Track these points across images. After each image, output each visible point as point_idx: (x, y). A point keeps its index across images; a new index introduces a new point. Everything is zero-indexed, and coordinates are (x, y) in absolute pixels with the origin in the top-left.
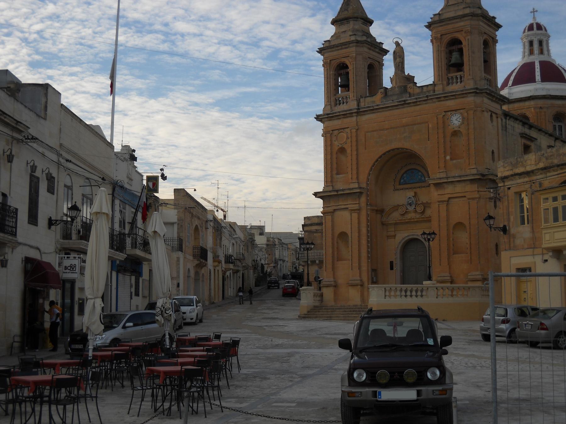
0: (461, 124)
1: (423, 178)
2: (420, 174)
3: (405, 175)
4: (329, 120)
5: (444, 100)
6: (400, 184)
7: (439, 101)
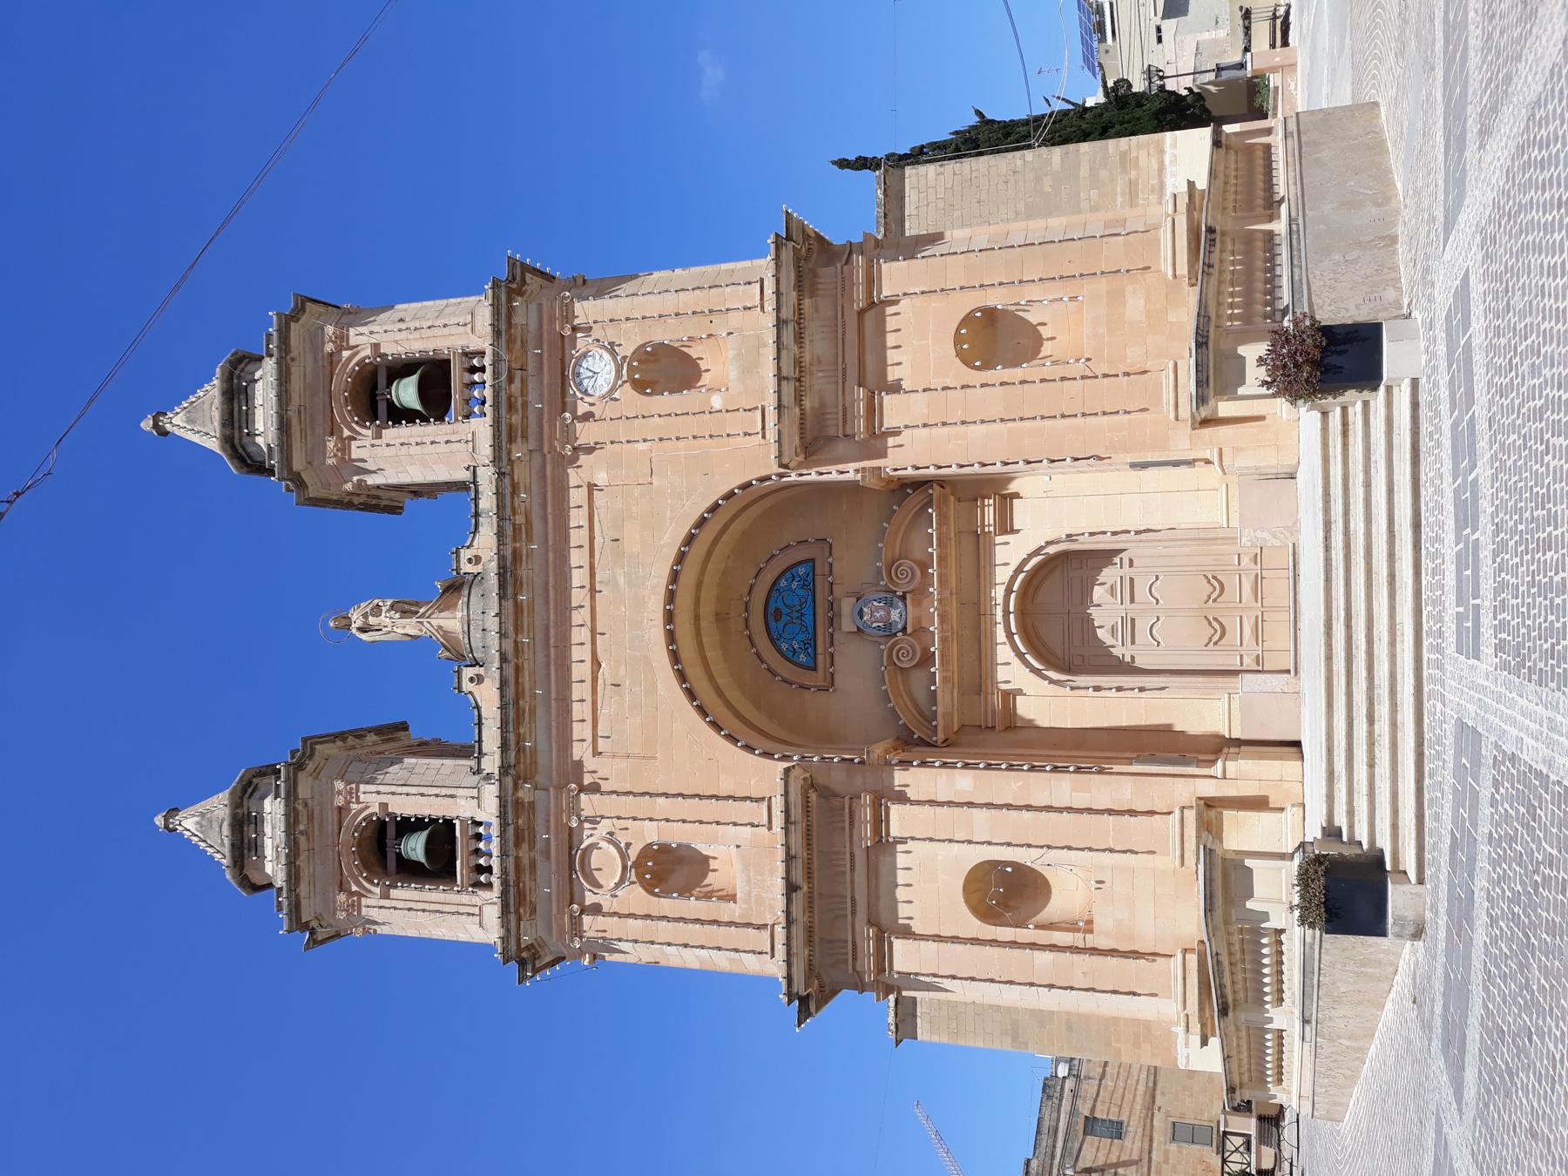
0: (613, 354)
1: (801, 571)
2: (783, 583)
3: (784, 646)
4: (533, 911)
5: (525, 417)
6: (815, 669)
7: (525, 437)
